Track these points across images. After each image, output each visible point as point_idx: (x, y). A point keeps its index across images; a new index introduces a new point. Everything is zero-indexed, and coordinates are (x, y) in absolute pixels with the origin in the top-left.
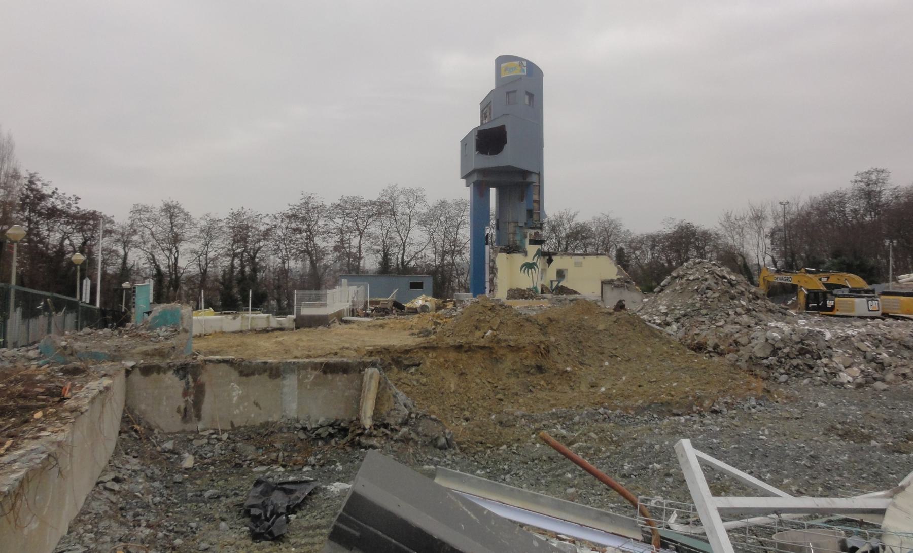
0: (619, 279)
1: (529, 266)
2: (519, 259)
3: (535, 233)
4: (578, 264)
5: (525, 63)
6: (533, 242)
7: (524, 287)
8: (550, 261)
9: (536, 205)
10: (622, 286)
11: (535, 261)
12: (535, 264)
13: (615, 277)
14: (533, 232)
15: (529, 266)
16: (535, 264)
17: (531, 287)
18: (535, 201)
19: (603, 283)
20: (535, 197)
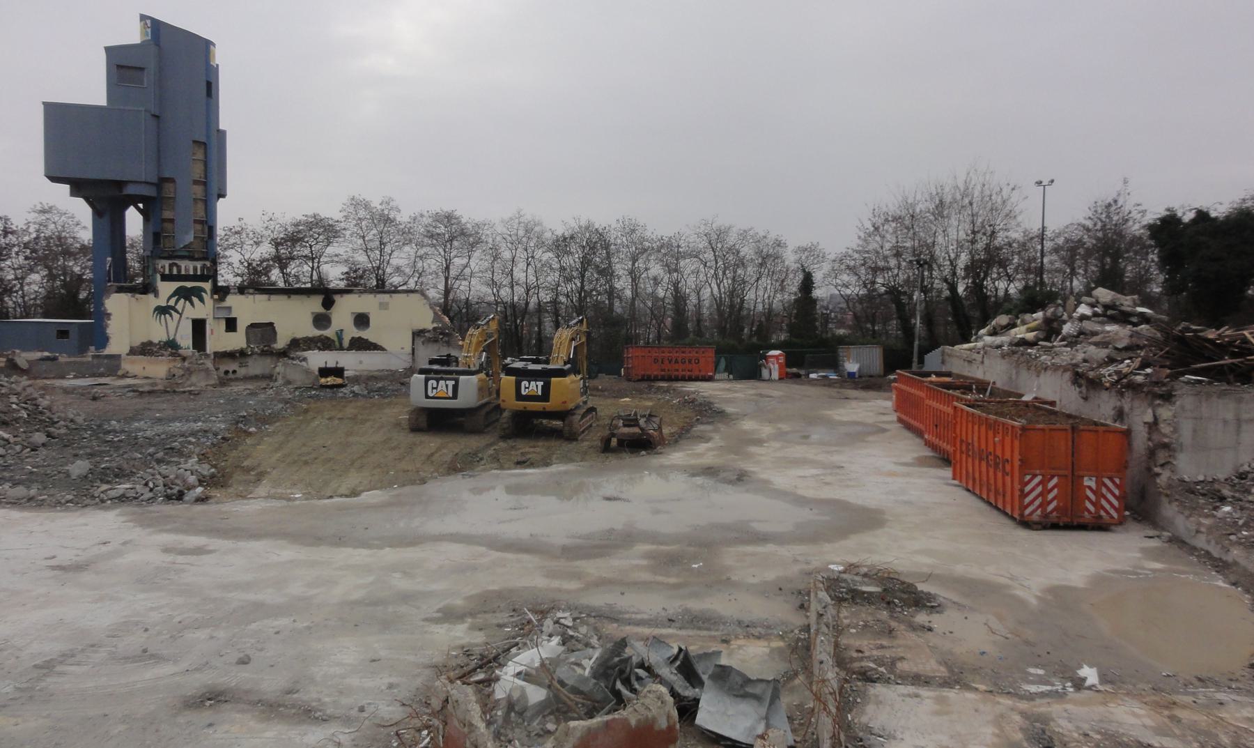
0: (435, 329)
1: (162, 311)
2: (151, 301)
3: (171, 266)
4: (384, 306)
5: (149, 22)
6: (165, 278)
7: (156, 341)
8: (328, 303)
9: (168, 226)
10: (436, 341)
11: (172, 303)
12: (173, 308)
13: (430, 326)
14: (166, 263)
15: (162, 311)
16: (173, 308)
17: (165, 339)
18: (164, 220)
19: (417, 334)
20: (167, 214)
